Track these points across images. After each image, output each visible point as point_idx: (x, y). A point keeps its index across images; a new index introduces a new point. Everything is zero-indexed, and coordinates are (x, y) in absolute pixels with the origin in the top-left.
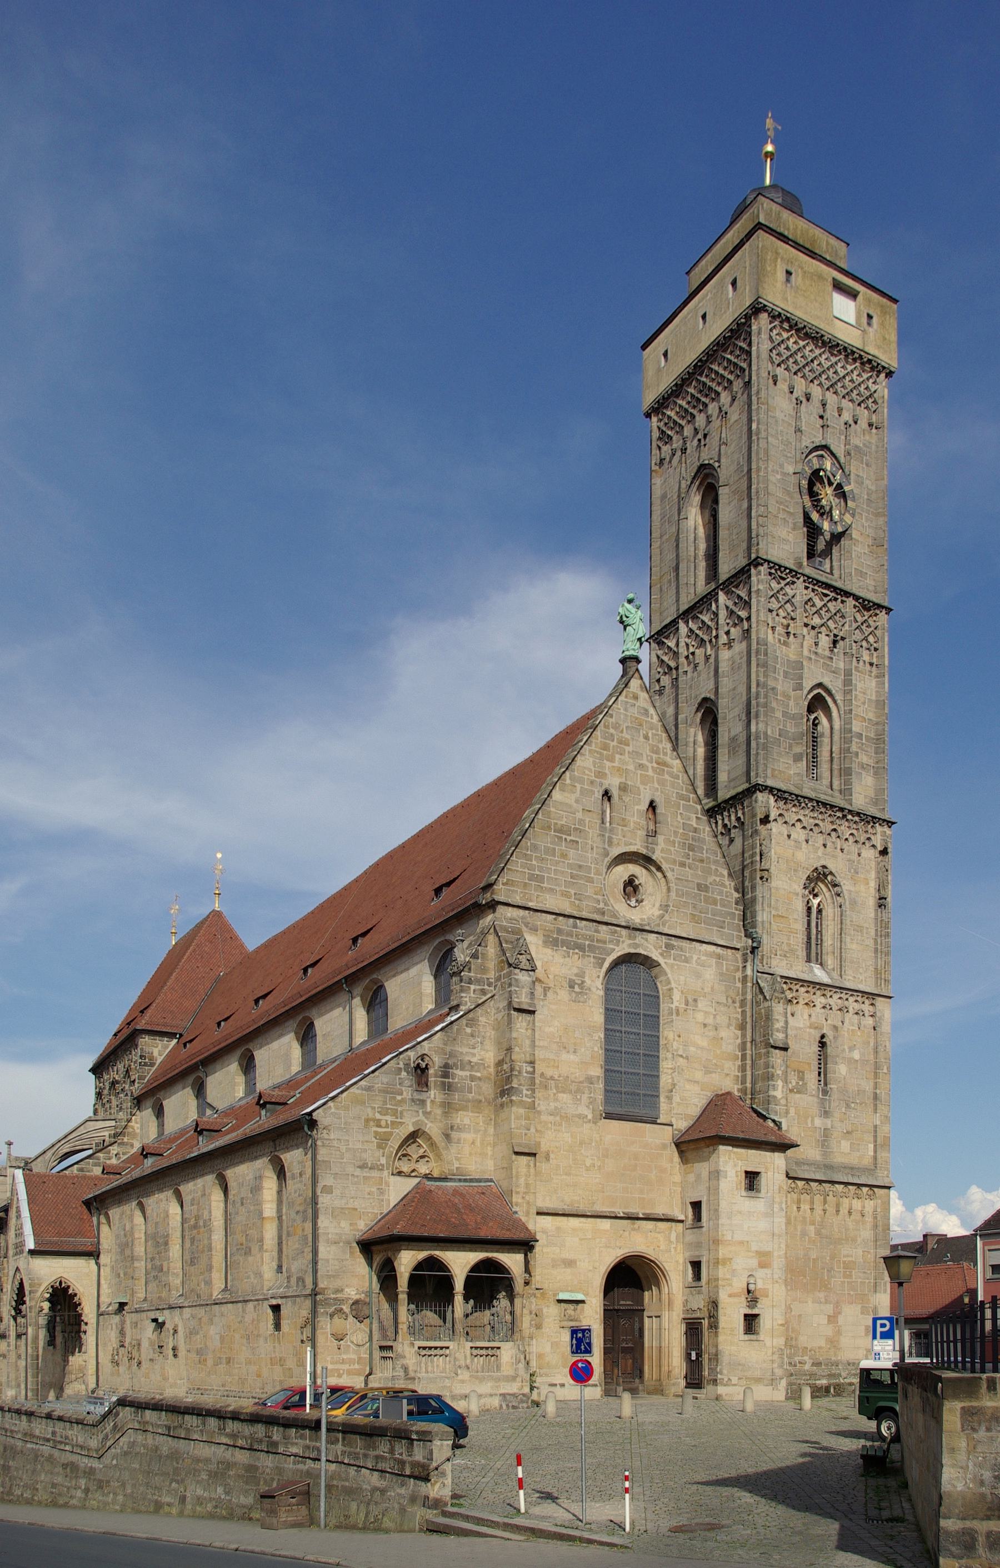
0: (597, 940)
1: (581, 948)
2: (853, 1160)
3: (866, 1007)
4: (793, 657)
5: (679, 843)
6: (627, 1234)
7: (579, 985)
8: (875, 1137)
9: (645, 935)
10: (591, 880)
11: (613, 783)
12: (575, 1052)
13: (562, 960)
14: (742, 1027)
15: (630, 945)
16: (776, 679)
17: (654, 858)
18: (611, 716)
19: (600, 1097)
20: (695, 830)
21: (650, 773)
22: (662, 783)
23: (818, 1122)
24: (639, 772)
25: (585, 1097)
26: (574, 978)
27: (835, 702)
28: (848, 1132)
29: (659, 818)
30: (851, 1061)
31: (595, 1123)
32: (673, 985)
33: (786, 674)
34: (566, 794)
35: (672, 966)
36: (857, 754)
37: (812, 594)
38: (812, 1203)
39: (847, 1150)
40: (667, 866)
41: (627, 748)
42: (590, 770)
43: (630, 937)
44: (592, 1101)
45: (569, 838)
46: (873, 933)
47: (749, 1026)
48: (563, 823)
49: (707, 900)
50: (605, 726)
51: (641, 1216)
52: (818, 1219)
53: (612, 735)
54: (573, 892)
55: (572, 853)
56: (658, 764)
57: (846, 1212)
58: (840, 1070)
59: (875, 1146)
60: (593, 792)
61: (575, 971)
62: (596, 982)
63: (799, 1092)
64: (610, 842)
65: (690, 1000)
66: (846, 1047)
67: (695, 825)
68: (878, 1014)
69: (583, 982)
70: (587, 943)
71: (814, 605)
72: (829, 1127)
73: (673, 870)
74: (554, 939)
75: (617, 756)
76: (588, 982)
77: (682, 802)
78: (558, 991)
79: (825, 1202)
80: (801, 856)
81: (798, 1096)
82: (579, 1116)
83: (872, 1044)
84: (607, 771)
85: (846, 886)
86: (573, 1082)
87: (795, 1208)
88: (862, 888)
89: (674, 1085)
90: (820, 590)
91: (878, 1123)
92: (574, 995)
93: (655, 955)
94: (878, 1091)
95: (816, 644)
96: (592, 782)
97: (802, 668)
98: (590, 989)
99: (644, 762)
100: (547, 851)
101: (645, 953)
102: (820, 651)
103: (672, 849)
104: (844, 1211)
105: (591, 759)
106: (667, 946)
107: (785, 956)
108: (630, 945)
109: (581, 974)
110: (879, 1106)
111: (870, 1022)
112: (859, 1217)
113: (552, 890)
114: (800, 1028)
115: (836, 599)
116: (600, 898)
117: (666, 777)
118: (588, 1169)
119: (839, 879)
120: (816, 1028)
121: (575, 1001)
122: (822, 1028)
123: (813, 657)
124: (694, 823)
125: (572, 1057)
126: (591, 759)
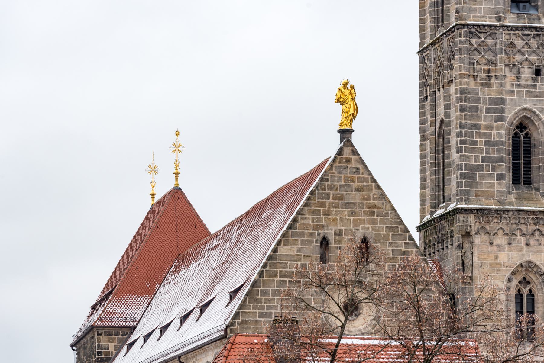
4: (494, 96)
16: (479, 117)
22: (373, 222)
24: (353, 218)
29: (371, 250)
33: (488, 110)
37: (514, 38)
56: (369, 207)
67: (403, 249)
71: (515, 46)
80: (503, 258)
90: (520, 33)
95: (518, 78)
97: (503, 101)
102: (523, 82)
115: (538, 35)
123: (515, 89)
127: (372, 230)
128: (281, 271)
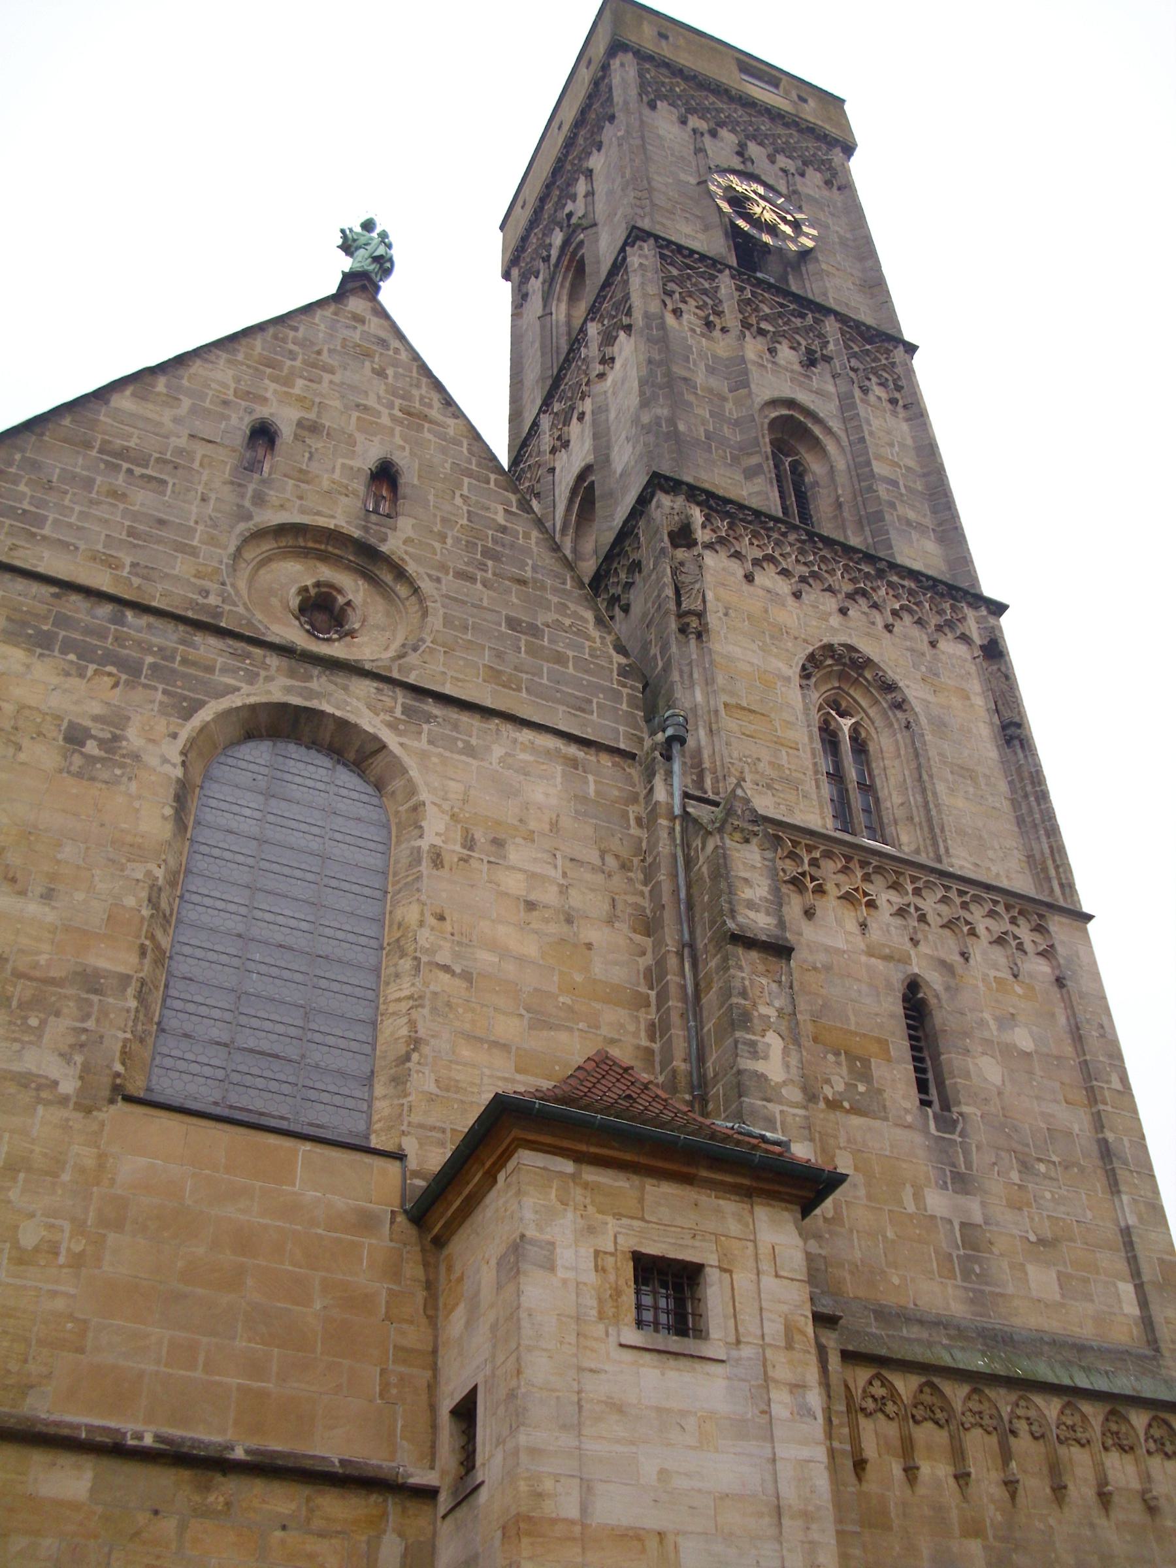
0: (185, 661)
1: (132, 669)
2: (1079, 1321)
3: (1024, 932)
5: (457, 540)
6: (169, 1525)
7: (101, 743)
8: (1133, 1261)
9: (341, 678)
10: (193, 552)
11: (286, 418)
12: (48, 896)
13: (55, 680)
14: (649, 926)
15: (288, 690)
17: (384, 548)
18: (296, 329)
19: (116, 1037)
20: (503, 529)
21: (385, 420)
23: (938, 1202)
25: (59, 1029)
26: (88, 723)
27: (829, 431)
28: (1041, 1241)
30: (1008, 1053)
31: (88, 1111)
32: (424, 796)
34: (150, 406)
35: (424, 756)
36: (892, 505)
38: (958, 1454)
39: (1053, 1293)
40: (421, 570)
41: (327, 377)
42: (227, 386)
43: (292, 674)
44: (83, 1043)
45: (138, 471)
46: (1003, 787)
47: (668, 916)
48: (132, 444)
49: (533, 651)
50: (275, 337)
51: (239, 1454)
52: (993, 1515)
53: (291, 352)
54: (128, 561)
55: (142, 498)
57: (1090, 1493)
58: (980, 1071)
59: (1139, 1288)
60: (228, 418)
61: (97, 708)
62: (159, 746)
63: (855, 1110)
64: (259, 499)
65: (479, 835)
66: (987, 1016)
68: (1060, 949)
69: (116, 738)
70: (150, 659)
72: (978, 1218)
73: (438, 580)
74: (40, 632)
75: (300, 382)
76: (134, 738)
77: (466, 480)
78: (26, 743)
79: (1006, 1455)
81: (855, 1121)
82: (24, 1080)
83: (1062, 1020)
84: (269, 395)
85: (914, 691)
86: (19, 975)
87: (897, 1470)
88: (956, 702)
89: (415, 1043)
91: (1132, 1220)
92: (77, 760)
93: (370, 722)
94: (1110, 1136)
96: (225, 403)
98: (136, 757)
99: (371, 402)
100: (70, 478)
101: (338, 713)
103: (437, 545)
104: (1081, 1490)
105: (230, 373)
106: (406, 710)
107: (769, 787)
108: (288, 690)
109: (117, 720)
110: (1122, 1174)
111: (1042, 968)
112: (1137, 1514)
113: (65, 545)
114: (839, 952)
116: (214, 587)
117: (427, 435)
118: (22, 1258)
119: (892, 675)
120: (887, 958)
121: (79, 775)
122: (905, 960)
124: (501, 519)
125: (33, 908)
126: (230, 373)
127: (412, 454)
128: (104, 442)
